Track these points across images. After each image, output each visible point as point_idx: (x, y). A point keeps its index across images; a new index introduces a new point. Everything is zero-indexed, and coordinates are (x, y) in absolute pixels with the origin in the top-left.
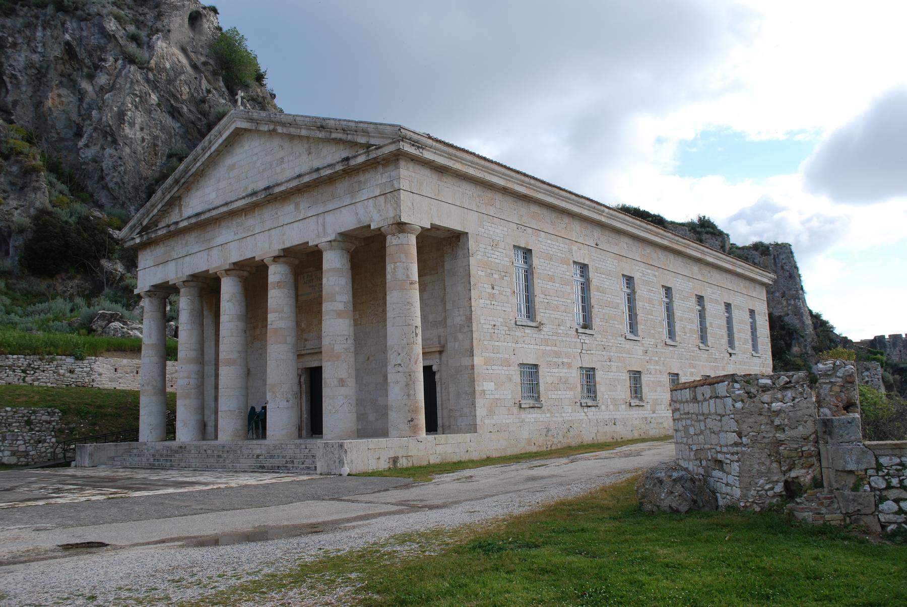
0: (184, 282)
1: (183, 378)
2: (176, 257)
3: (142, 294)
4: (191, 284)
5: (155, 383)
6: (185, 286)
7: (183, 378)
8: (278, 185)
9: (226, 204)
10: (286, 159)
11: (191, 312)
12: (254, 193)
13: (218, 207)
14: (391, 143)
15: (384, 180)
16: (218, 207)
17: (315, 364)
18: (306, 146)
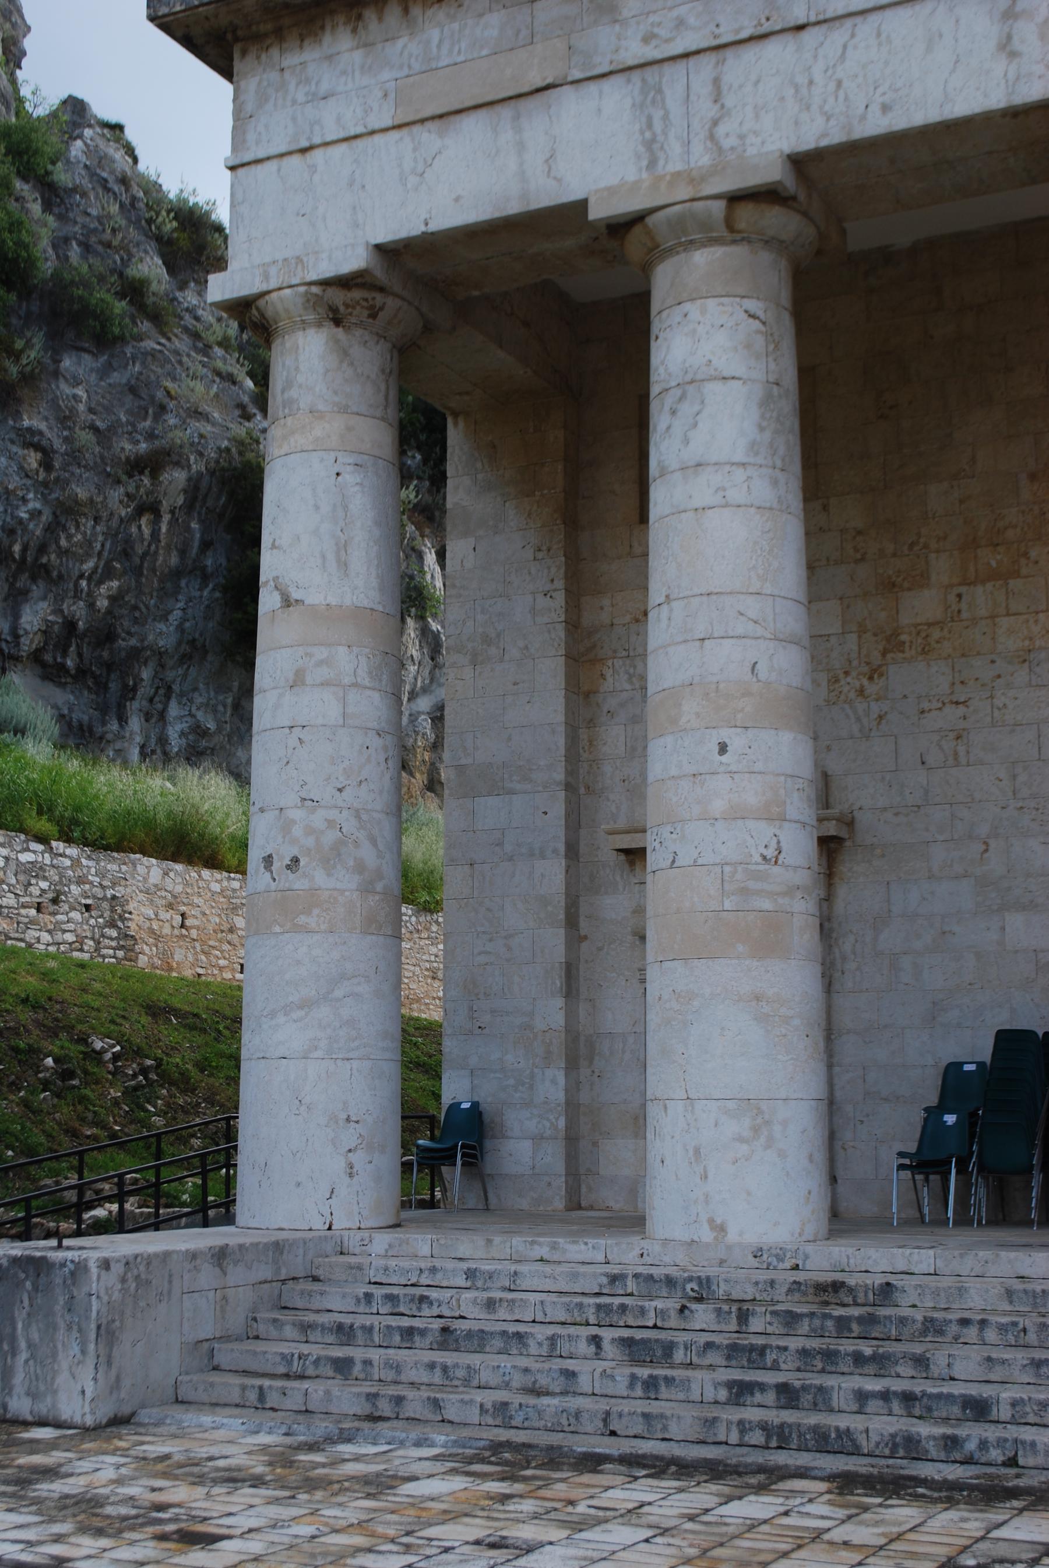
0: (735, 199)
1: (736, 814)
2: (635, 51)
3: (285, 303)
4: (776, 220)
5: (368, 854)
6: (732, 232)
7: (736, 814)
11: (766, 401)
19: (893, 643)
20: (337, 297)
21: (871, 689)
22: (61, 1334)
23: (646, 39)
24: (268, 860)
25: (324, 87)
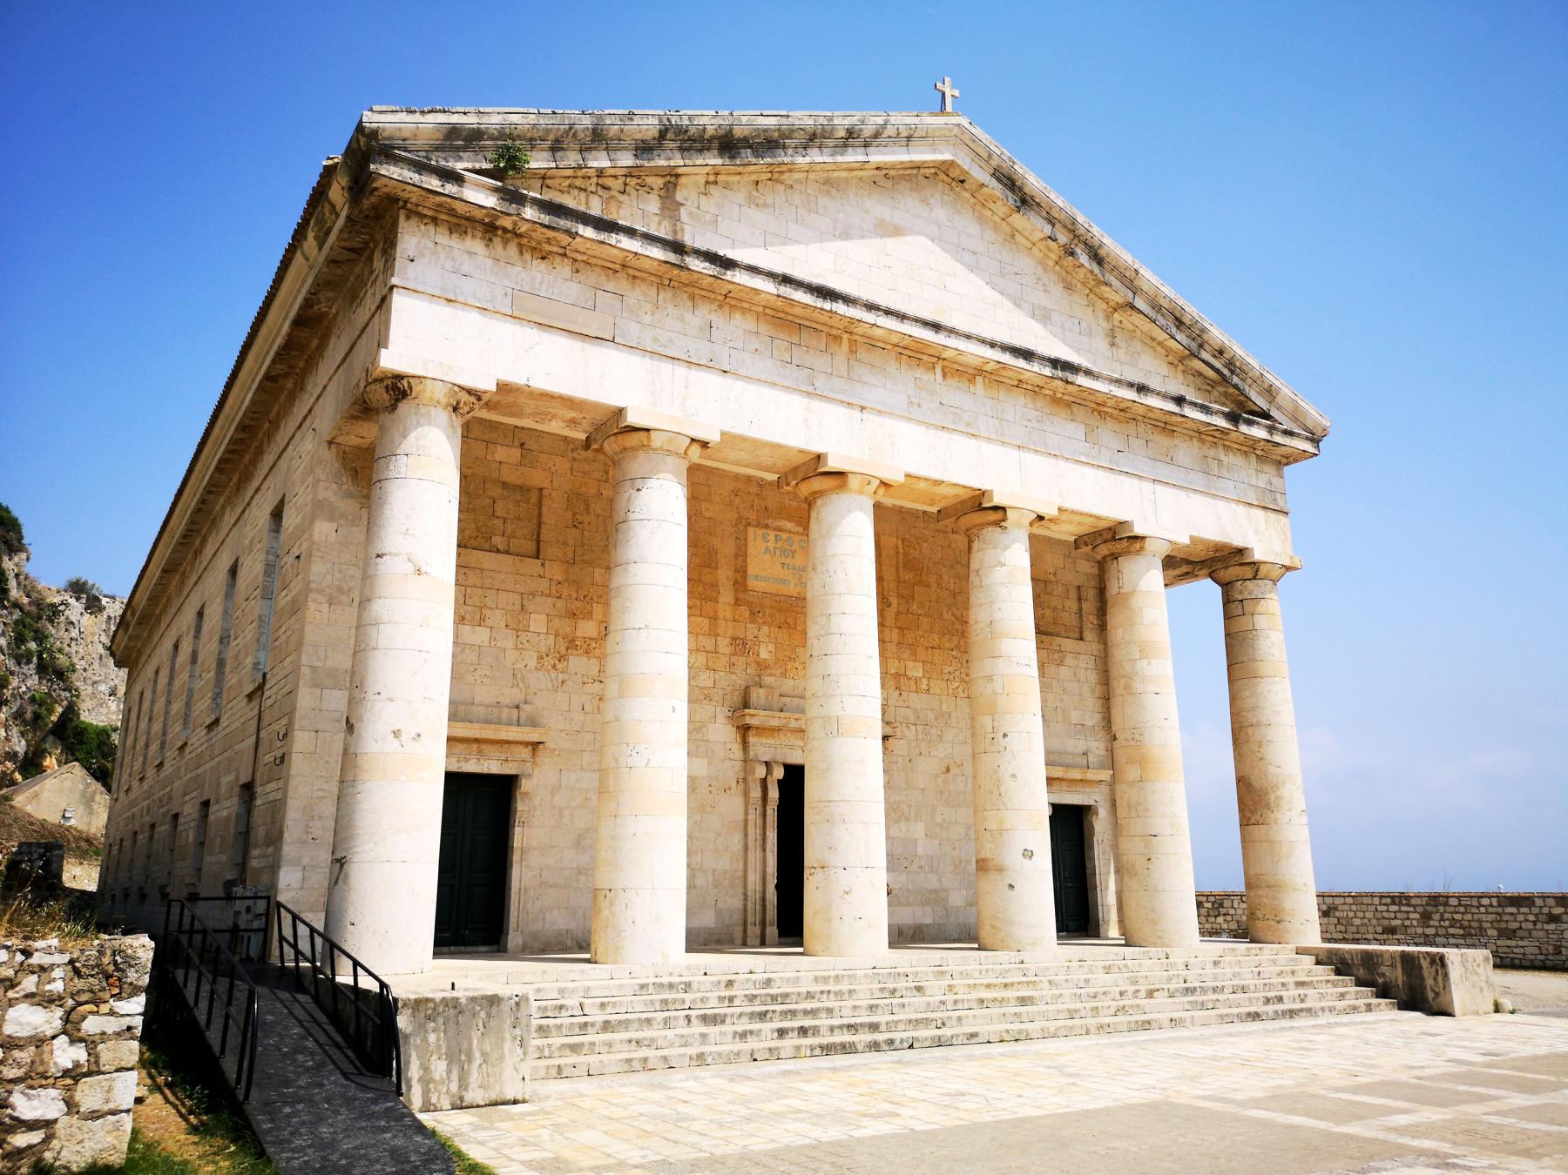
9: (936, 327)
10: (1055, 316)
13: (903, 317)
14: (1307, 438)
15: (1262, 484)
16: (903, 317)
17: (795, 759)
18: (1105, 325)
19: (572, 644)
20: (464, 397)
21: (559, 666)
22: (507, 1045)
23: (655, 340)
24: (397, 734)
25: (465, 269)
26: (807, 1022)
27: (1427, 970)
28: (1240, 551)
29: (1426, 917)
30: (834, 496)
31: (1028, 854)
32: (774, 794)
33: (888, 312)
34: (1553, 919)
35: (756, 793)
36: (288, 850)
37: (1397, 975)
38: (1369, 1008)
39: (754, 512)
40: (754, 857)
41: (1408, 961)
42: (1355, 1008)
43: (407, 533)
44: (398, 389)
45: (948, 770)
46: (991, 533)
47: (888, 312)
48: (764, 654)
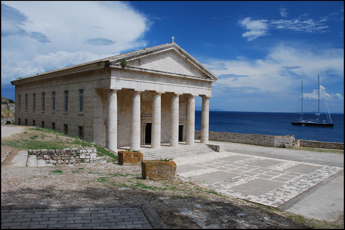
8: (188, 76)
12: (181, 75)
16: (166, 73)
19: (122, 110)
24: (113, 129)
26: (154, 157)
27: (218, 147)
28: (205, 95)
29: (225, 136)
30: (157, 95)
31: (176, 136)
32: (145, 127)
33: (164, 72)
34: (239, 137)
35: (143, 127)
36: (94, 137)
37: (215, 148)
38: (211, 151)
39: (148, 98)
40: (143, 135)
41: (216, 146)
42: (209, 152)
43: (113, 107)
44: (112, 91)
45: (166, 122)
46: (174, 97)
47: (164, 72)
48: (144, 109)
